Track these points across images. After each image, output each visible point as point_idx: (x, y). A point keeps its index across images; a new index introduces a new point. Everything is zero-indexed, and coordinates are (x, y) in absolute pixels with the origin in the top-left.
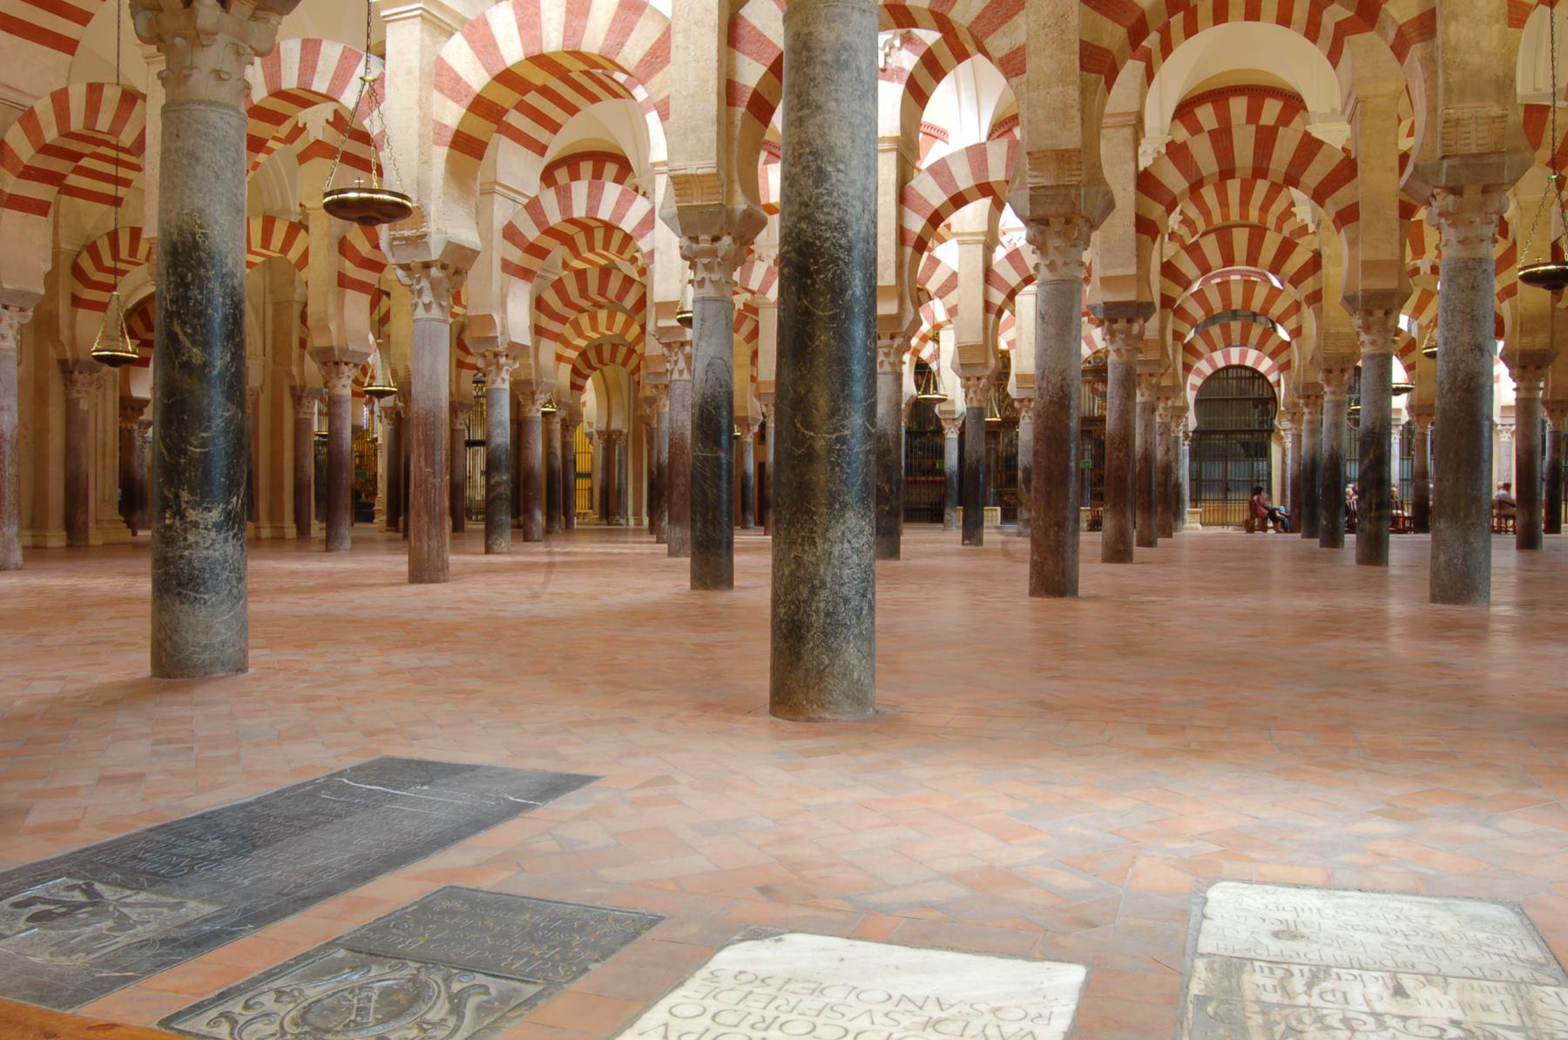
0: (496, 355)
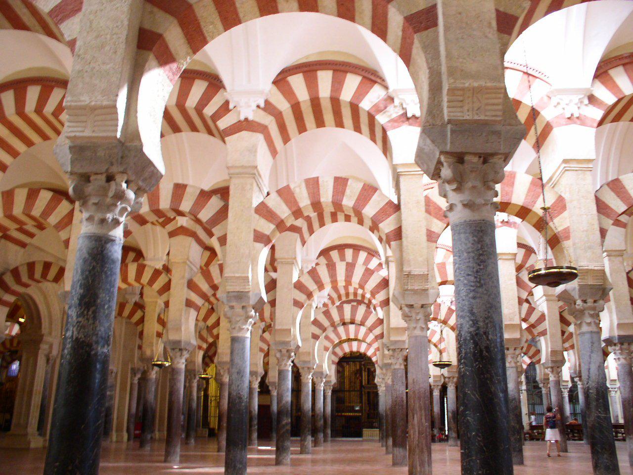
0: (288, 351)
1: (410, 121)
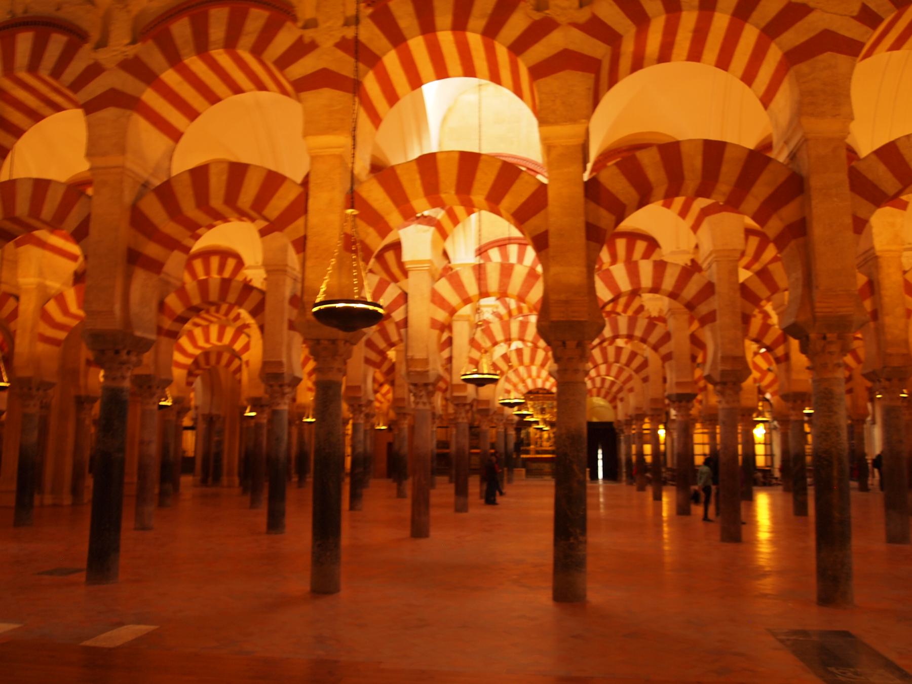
0: (360, 406)
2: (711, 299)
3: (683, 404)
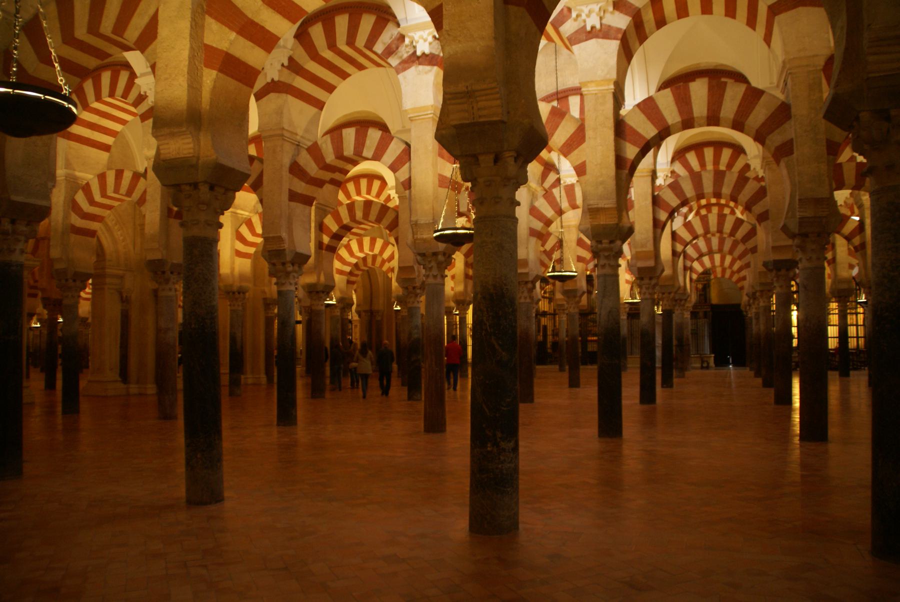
0: (414, 288)
1: (420, 59)
2: (786, 126)
3: (783, 272)
